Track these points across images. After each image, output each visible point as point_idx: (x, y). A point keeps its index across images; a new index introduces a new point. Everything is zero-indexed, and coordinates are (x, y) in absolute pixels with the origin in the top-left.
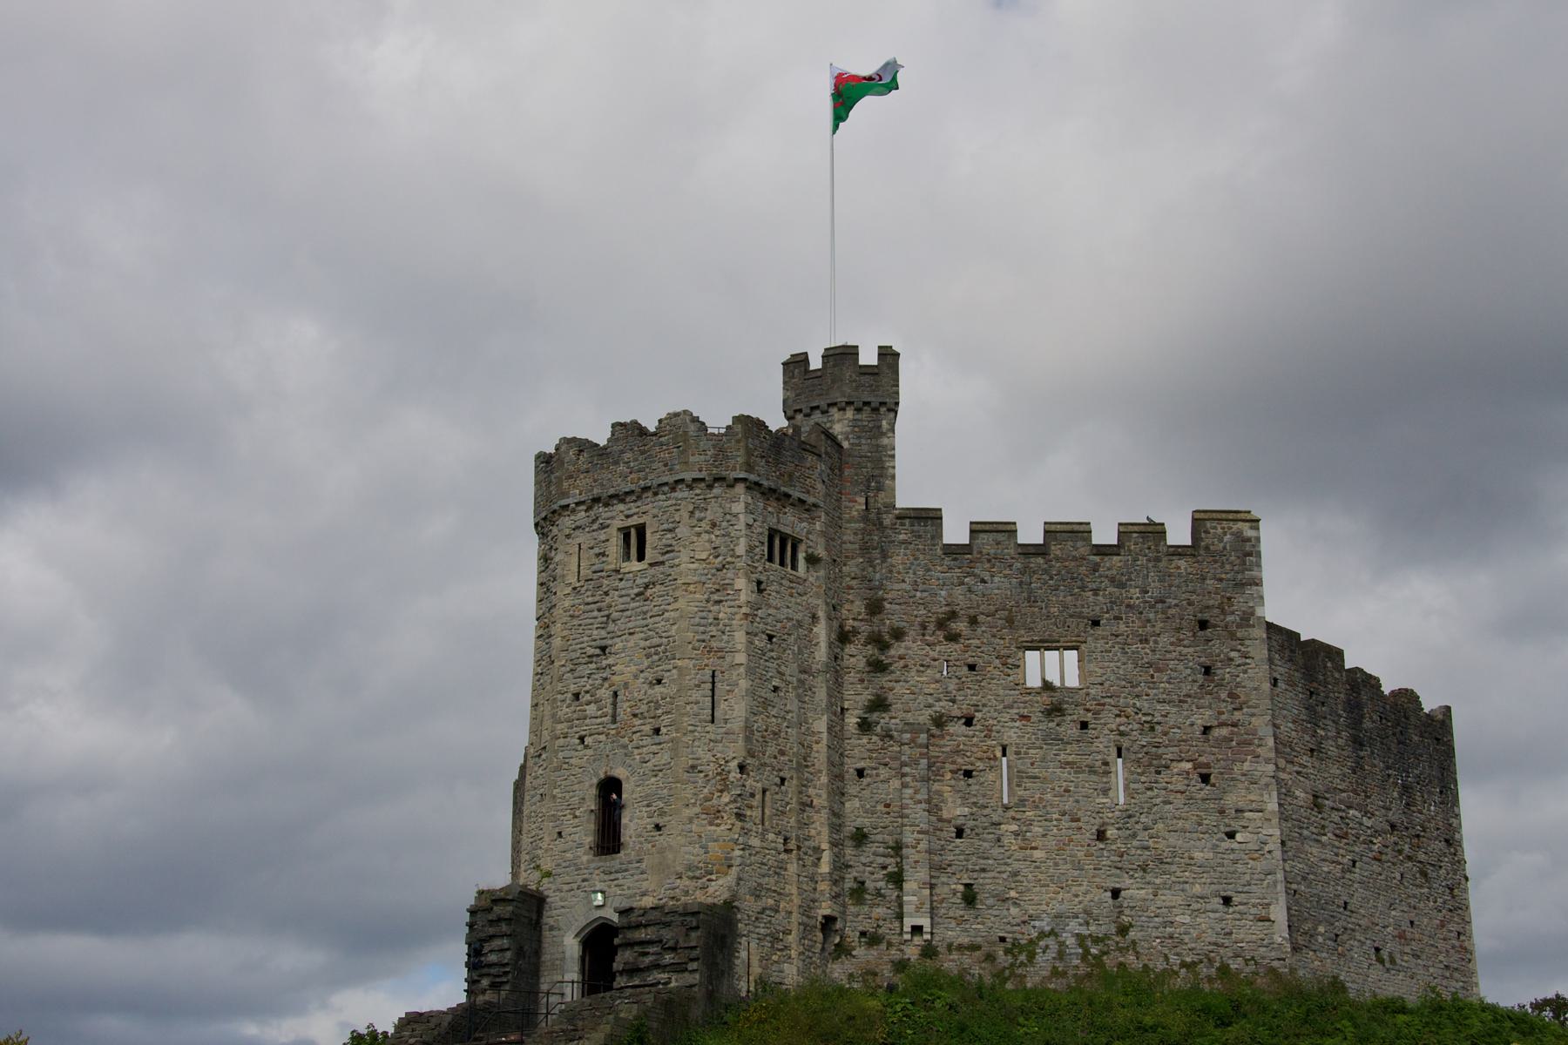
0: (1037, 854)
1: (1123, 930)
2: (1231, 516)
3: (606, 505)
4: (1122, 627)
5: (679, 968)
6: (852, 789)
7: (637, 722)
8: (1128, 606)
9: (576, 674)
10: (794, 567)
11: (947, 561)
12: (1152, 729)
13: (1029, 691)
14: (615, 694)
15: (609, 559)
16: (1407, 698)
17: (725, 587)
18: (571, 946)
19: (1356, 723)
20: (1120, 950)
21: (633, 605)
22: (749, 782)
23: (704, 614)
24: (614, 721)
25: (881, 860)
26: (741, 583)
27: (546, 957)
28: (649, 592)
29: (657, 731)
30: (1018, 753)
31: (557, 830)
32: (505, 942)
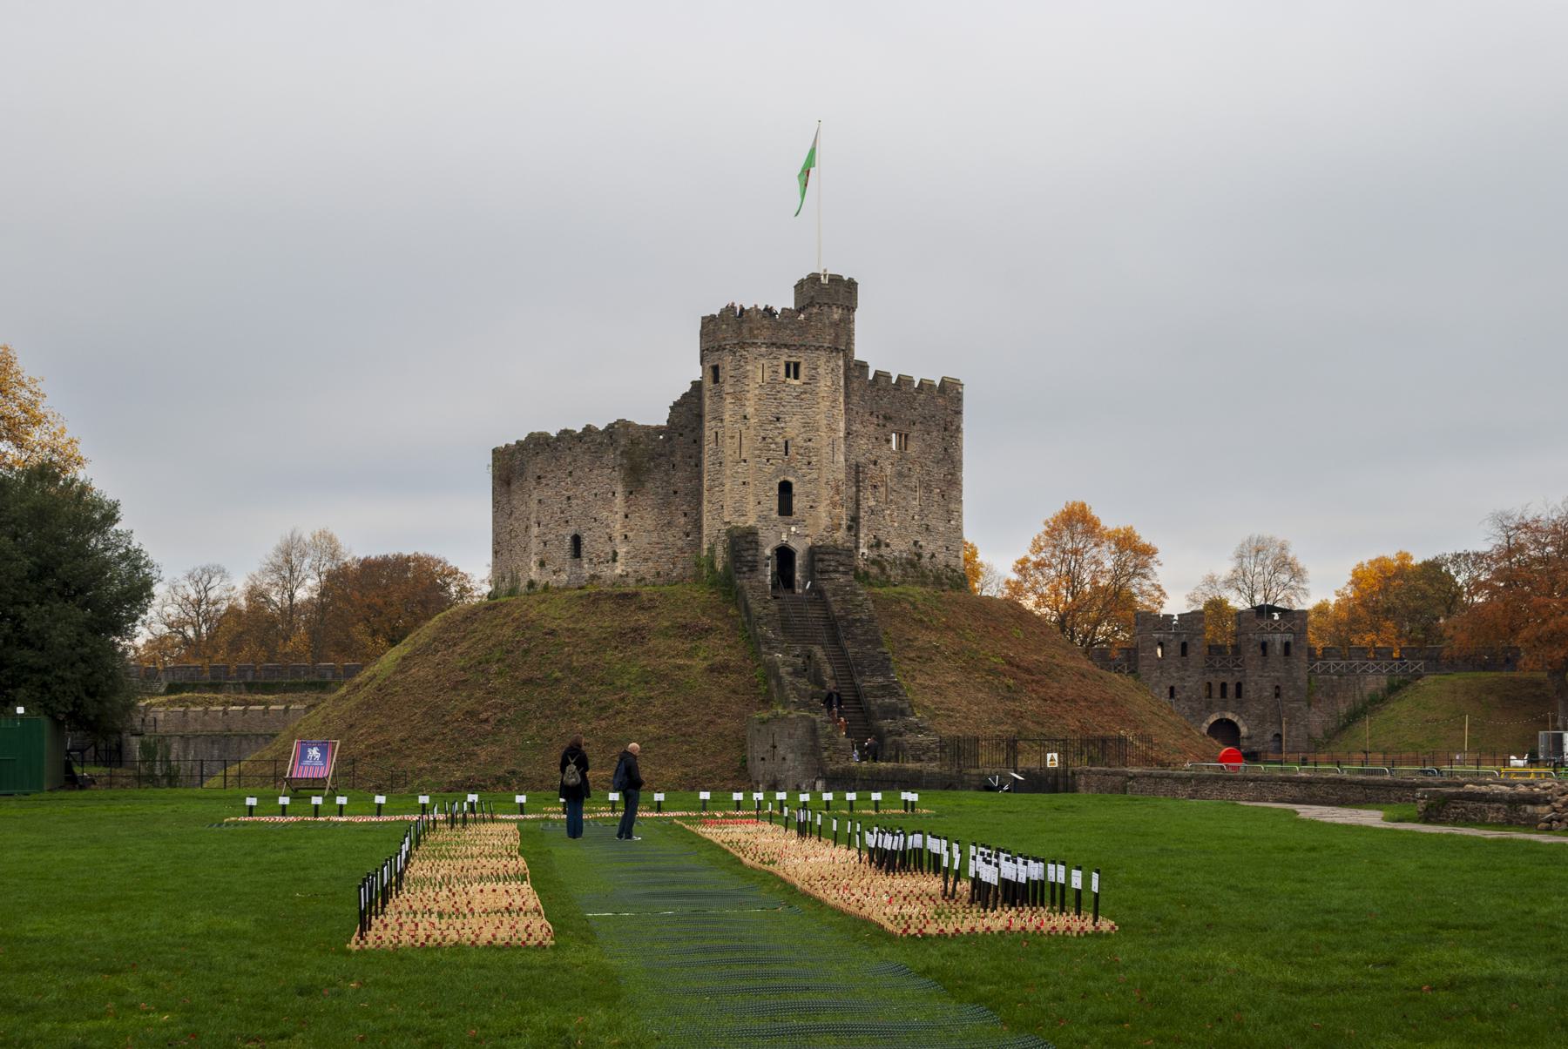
0: (896, 524)
3: (778, 347)
8: (925, 418)
13: (893, 452)
14: (786, 442)
15: (781, 375)
18: (768, 552)
24: (786, 454)
28: (803, 396)
29: (809, 463)
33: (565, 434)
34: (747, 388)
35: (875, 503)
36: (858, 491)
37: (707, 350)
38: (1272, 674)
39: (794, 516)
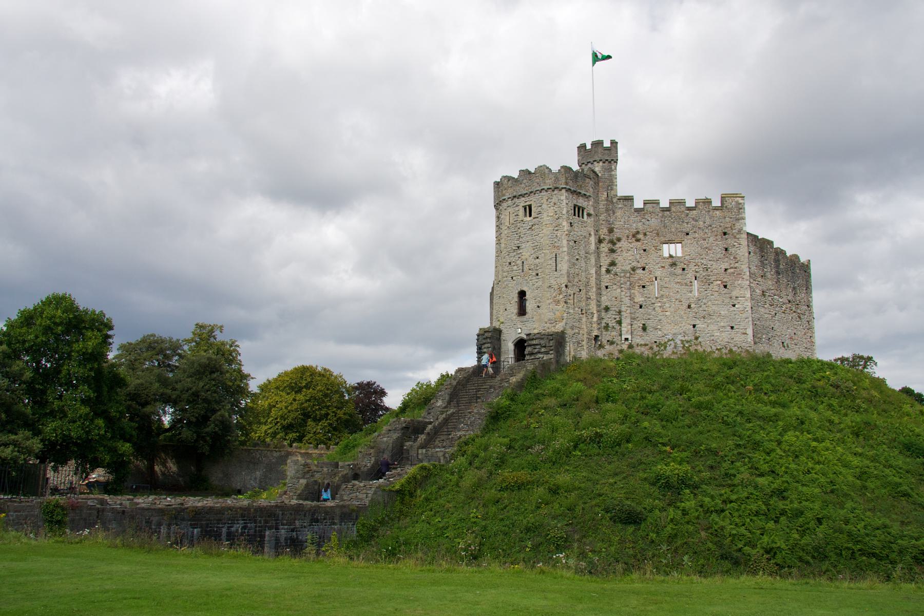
0: (667, 313)
1: (697, 338)
2: (735, 196)
3: (518, 198)
4: (697, 235)
5: (547, 353)
6: (604, 292)
7: (530, 271)
10: (583, 217)
11: (636, 214)
12: (707, 270)
13: (664, 258)
14: (523, 262)
16: (796, 257)
17: (559, 225)
19: (777, 266)
20: (696, 345)
21: (528, 232)
22: (569, 291)
25: (614, 316)
26: (565, 224)
27: (502, 350)
28: (533, 228)
29: (537, 275)
32: (489, 345)
35: (643, 299)
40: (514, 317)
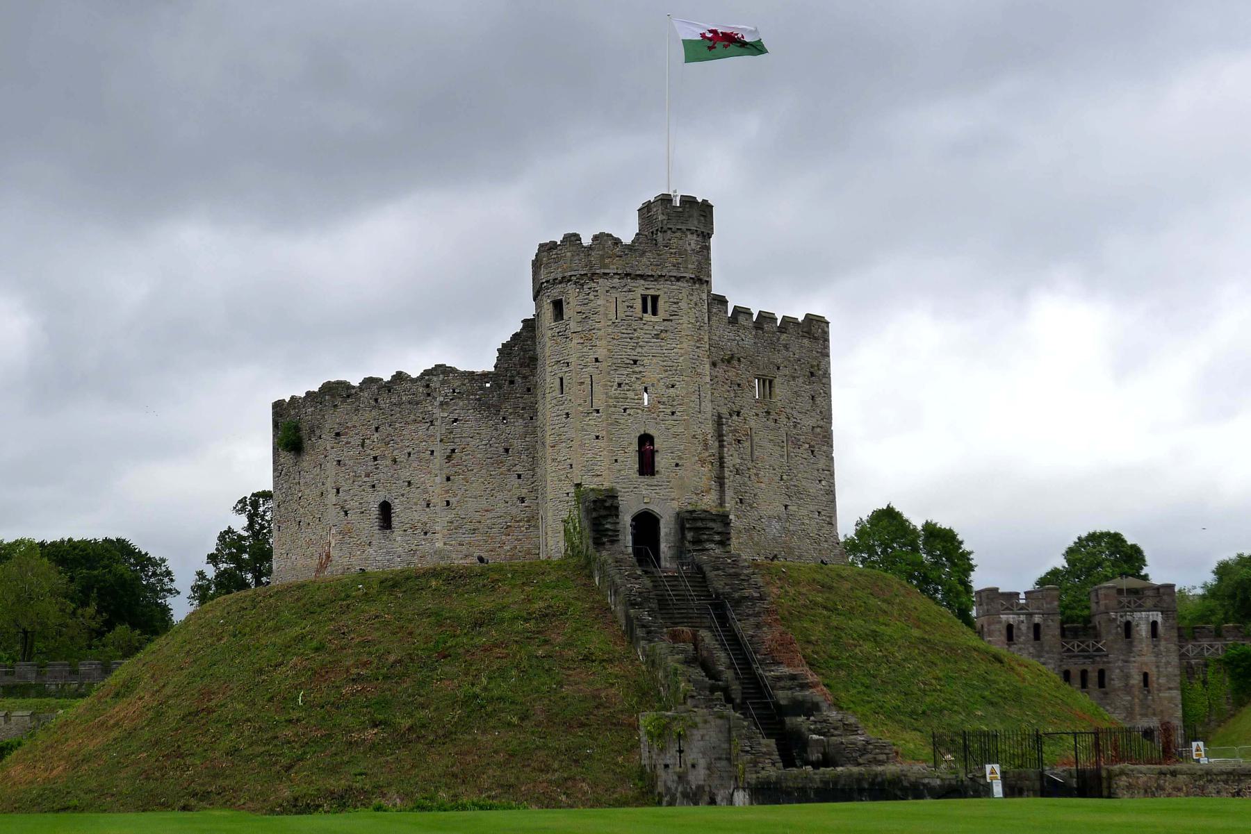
3: (632, 279)
9: (618, 372)
13: (757, 401)
15: (637, 310)
18: (626, 519)
23: (694, 353)
28: (663, 335)
29: (673, 413)
30: (755, 433)
31: (615, 458)
33: (369, 381)
34: (598, 326)
35: (739, 461)
36: (721, 446)
37: (547, 282)
38: (1138, 659)
39: (657, 476)
40: (635, 476)
